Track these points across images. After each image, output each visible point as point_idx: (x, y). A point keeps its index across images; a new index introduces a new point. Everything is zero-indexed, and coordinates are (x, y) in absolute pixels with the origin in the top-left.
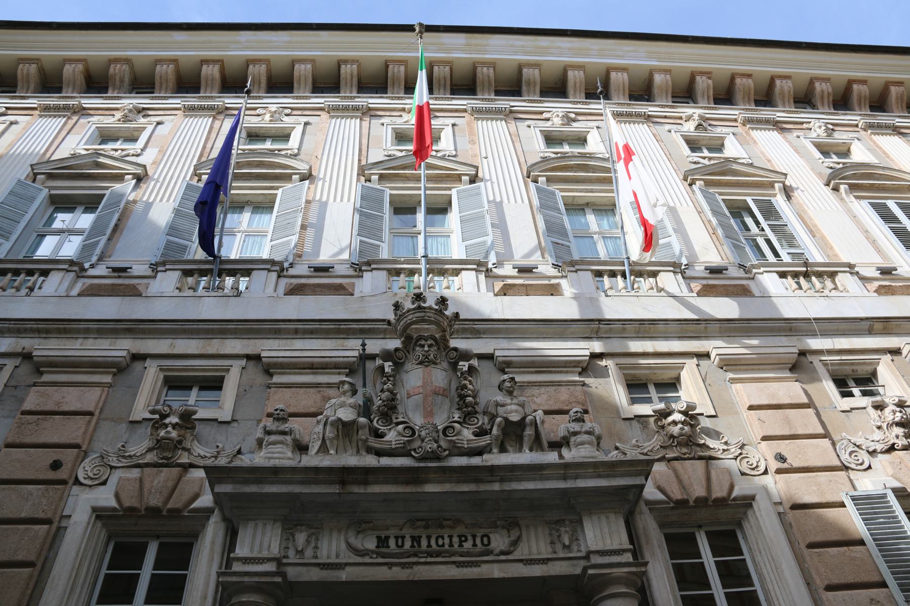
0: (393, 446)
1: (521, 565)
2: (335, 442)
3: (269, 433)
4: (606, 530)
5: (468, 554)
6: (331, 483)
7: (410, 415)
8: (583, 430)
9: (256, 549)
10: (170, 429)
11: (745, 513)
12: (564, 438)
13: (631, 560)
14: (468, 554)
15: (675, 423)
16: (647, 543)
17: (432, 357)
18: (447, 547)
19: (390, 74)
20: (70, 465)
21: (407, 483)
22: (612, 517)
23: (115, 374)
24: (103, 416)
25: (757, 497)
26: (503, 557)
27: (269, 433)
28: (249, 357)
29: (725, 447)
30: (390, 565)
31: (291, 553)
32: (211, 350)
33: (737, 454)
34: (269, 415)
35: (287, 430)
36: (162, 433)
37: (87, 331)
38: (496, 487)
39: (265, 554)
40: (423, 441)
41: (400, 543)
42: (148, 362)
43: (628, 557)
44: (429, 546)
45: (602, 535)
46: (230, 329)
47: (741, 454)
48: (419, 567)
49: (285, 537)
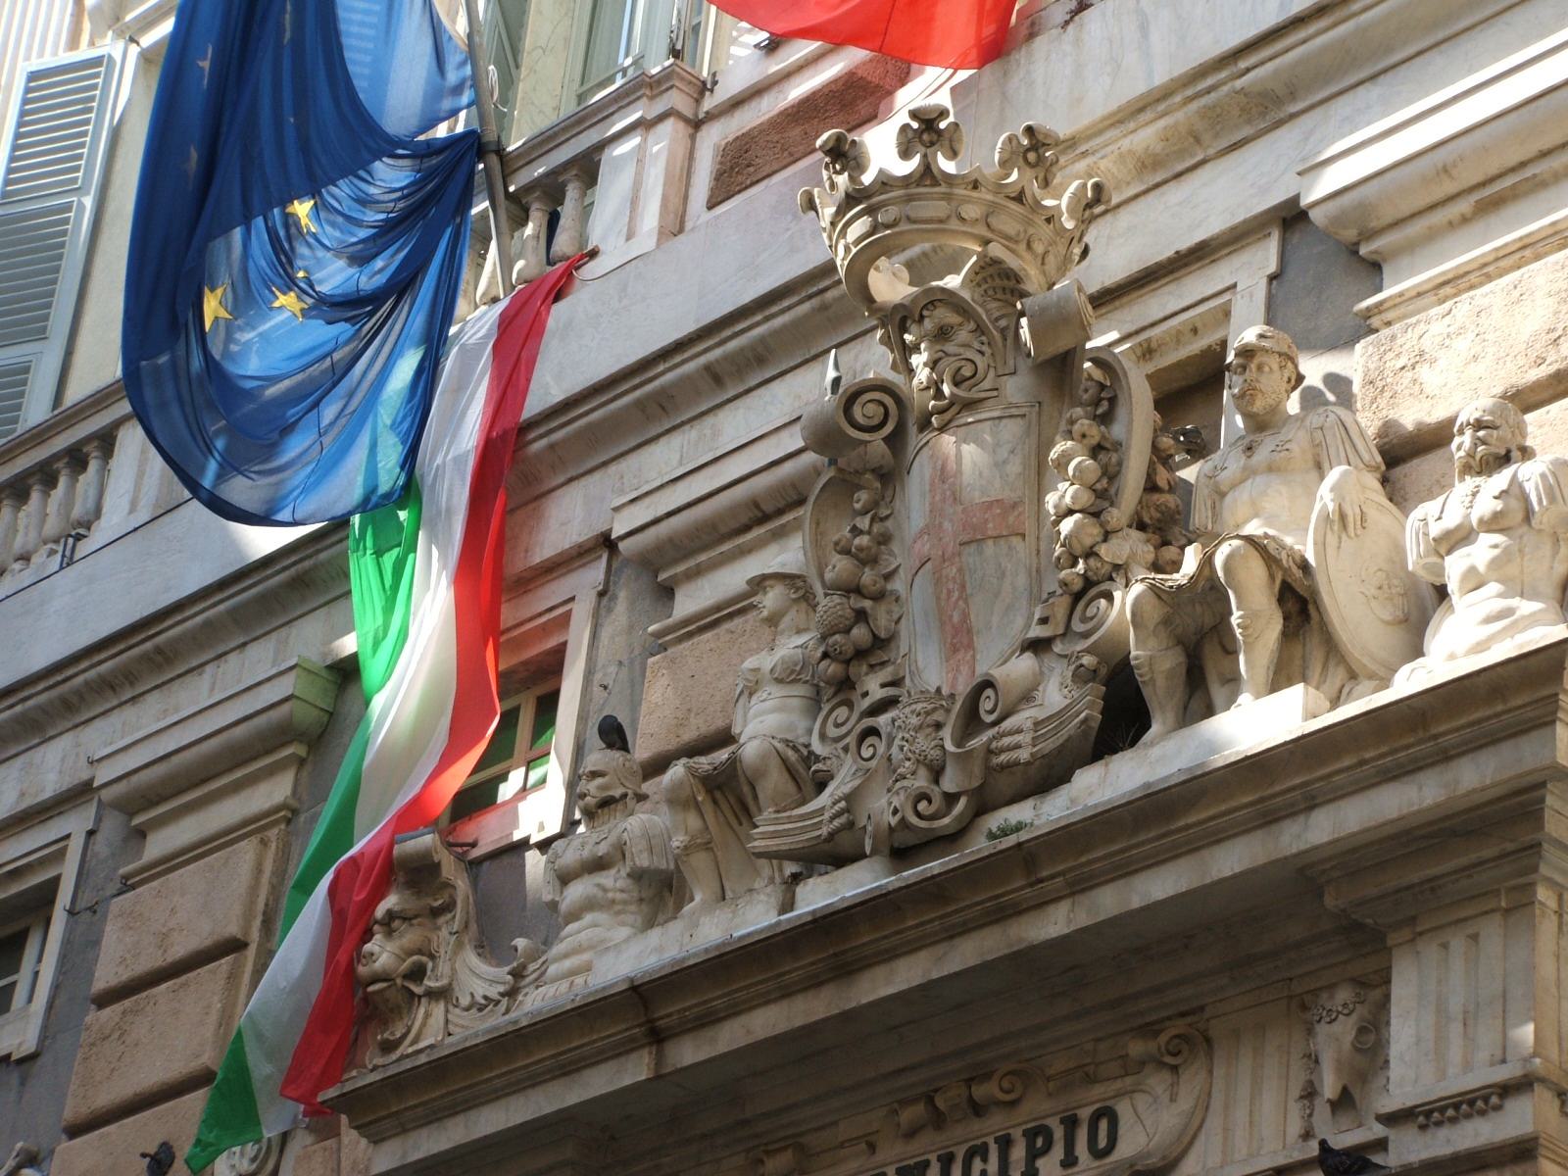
0: (824, 831)
2: (700, 861)
6: (620, 1051)
21: (813, 983)
37: (210, 632)
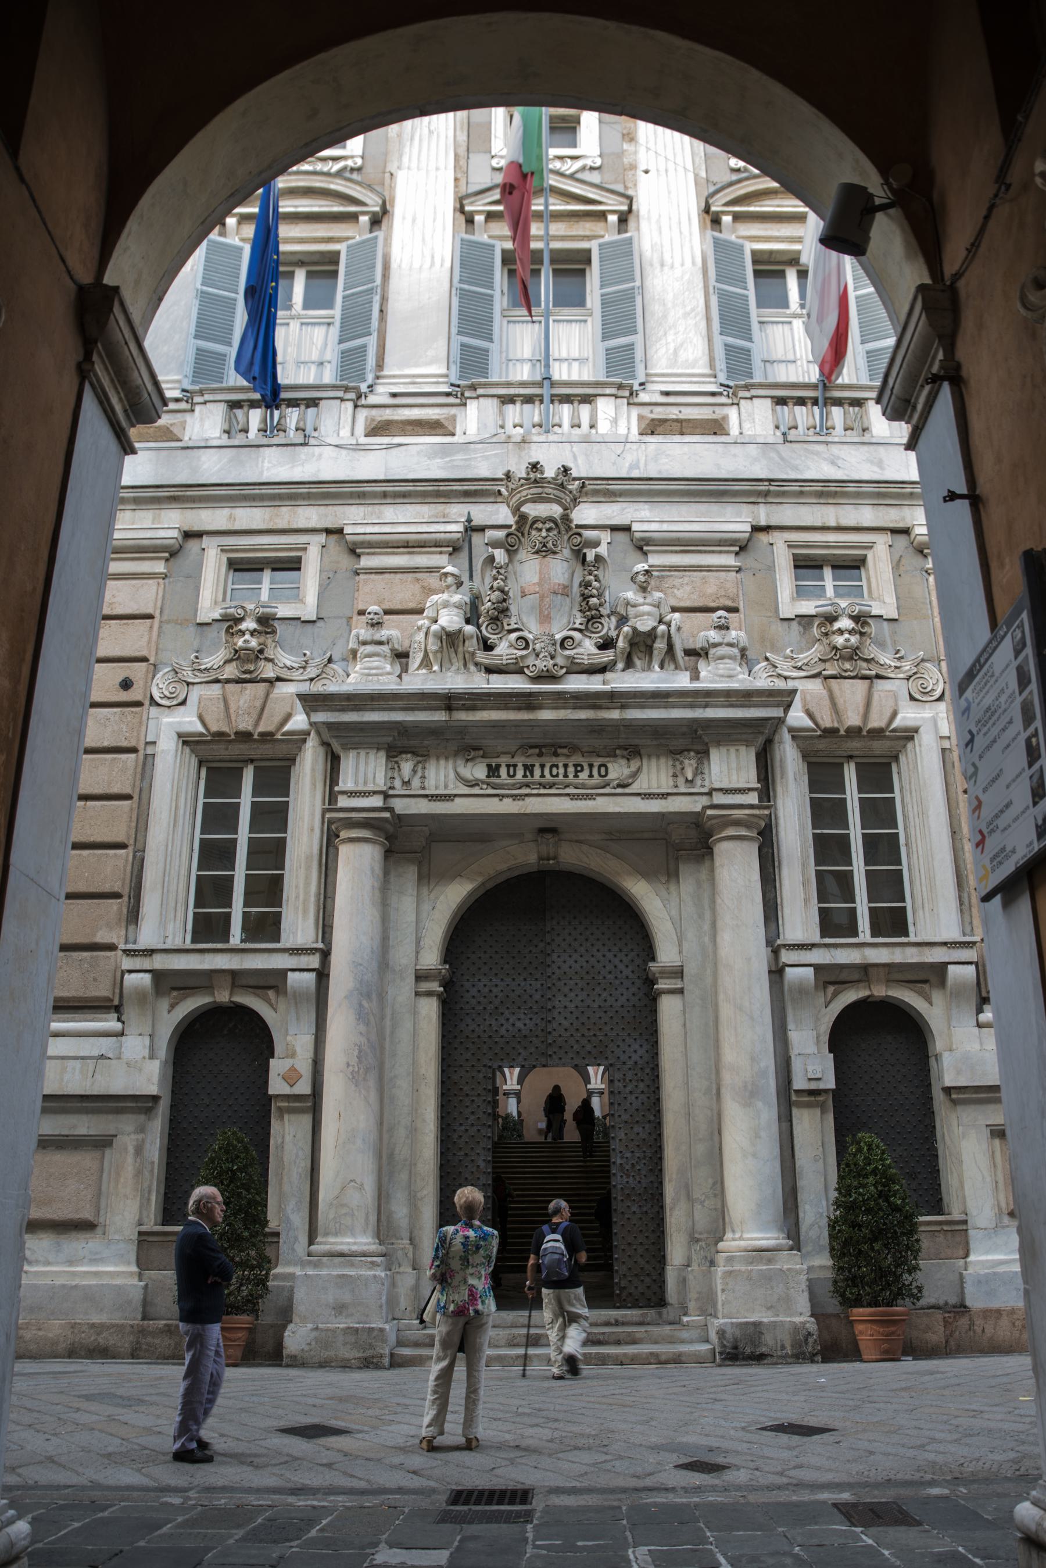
0: (505, 662)
1: (639, 798)
2: (439, 655)
3: (365, 643)
4: (734, 765)
5: (584, 786)
7: (525, 620)
8: (725, 641)
9: (361, 781)
10: (247, 637)
11: (905, 746)
12: (702, 649)
13: (756, 801)
14: (584, 786)
15: (841, 632)
16: (782, 778)
17: (550, 545)
18: (561, 777)
20: (141, 683)
21: (519, 709)
22: (743, 749)
23: (167, 560)
24: (165, 618)
25: (921, 730)
26: (619, 790)
27: (365, 643)
28: (328, 531)
29: (898, 664)
30: (501, 797)
31: (397, 783)
32: (282, 524)
33: (910, 673)
34: (361, 613)
35: (384, 639)
36: (240, 642)
38: (615, 714)
39: (371, 787)
40: (537, 655)
41: (512, 773)
42: (206, 541)
43: (753, 798)
44: (543, 776)
45: (730, 770)
46: (301, 494)
47: (915, 673)
48: (531, 799)
49: (390, 766)
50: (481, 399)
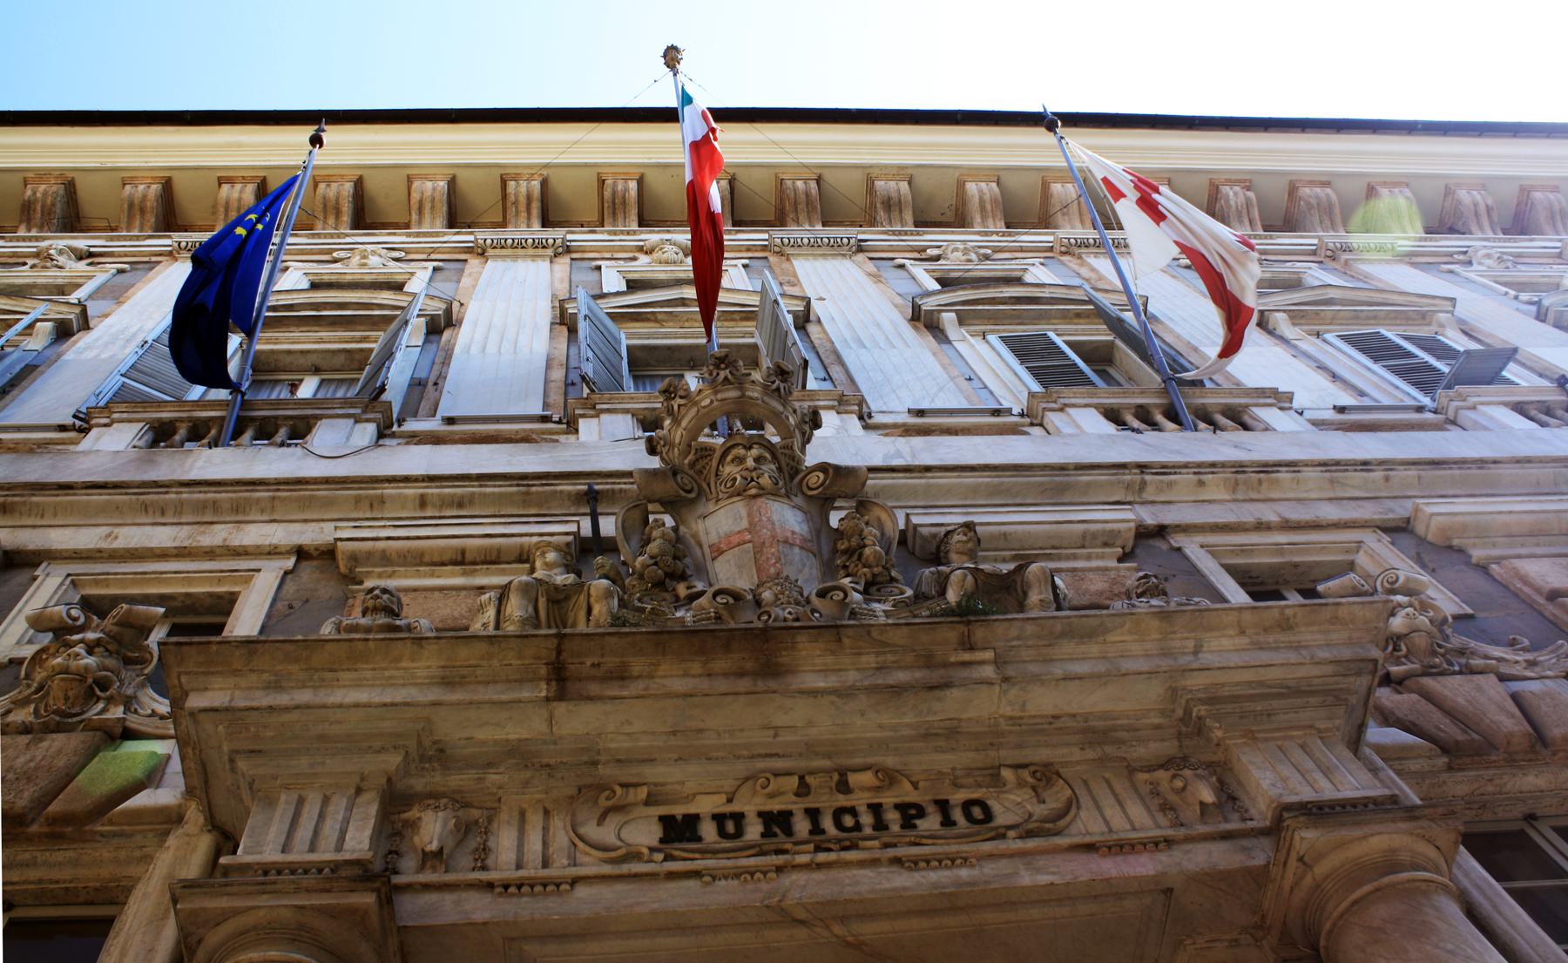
19: (607, 194)
50: (604, 417)
